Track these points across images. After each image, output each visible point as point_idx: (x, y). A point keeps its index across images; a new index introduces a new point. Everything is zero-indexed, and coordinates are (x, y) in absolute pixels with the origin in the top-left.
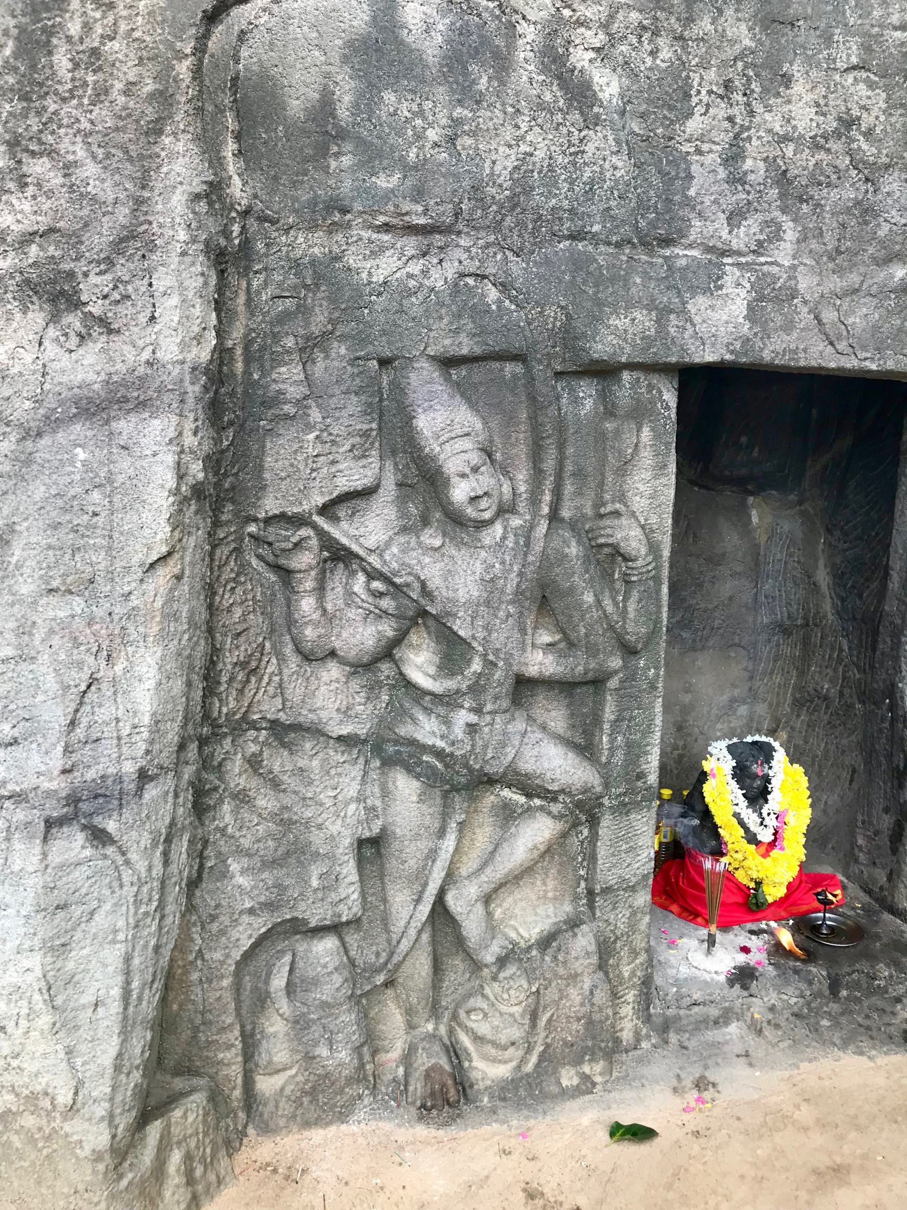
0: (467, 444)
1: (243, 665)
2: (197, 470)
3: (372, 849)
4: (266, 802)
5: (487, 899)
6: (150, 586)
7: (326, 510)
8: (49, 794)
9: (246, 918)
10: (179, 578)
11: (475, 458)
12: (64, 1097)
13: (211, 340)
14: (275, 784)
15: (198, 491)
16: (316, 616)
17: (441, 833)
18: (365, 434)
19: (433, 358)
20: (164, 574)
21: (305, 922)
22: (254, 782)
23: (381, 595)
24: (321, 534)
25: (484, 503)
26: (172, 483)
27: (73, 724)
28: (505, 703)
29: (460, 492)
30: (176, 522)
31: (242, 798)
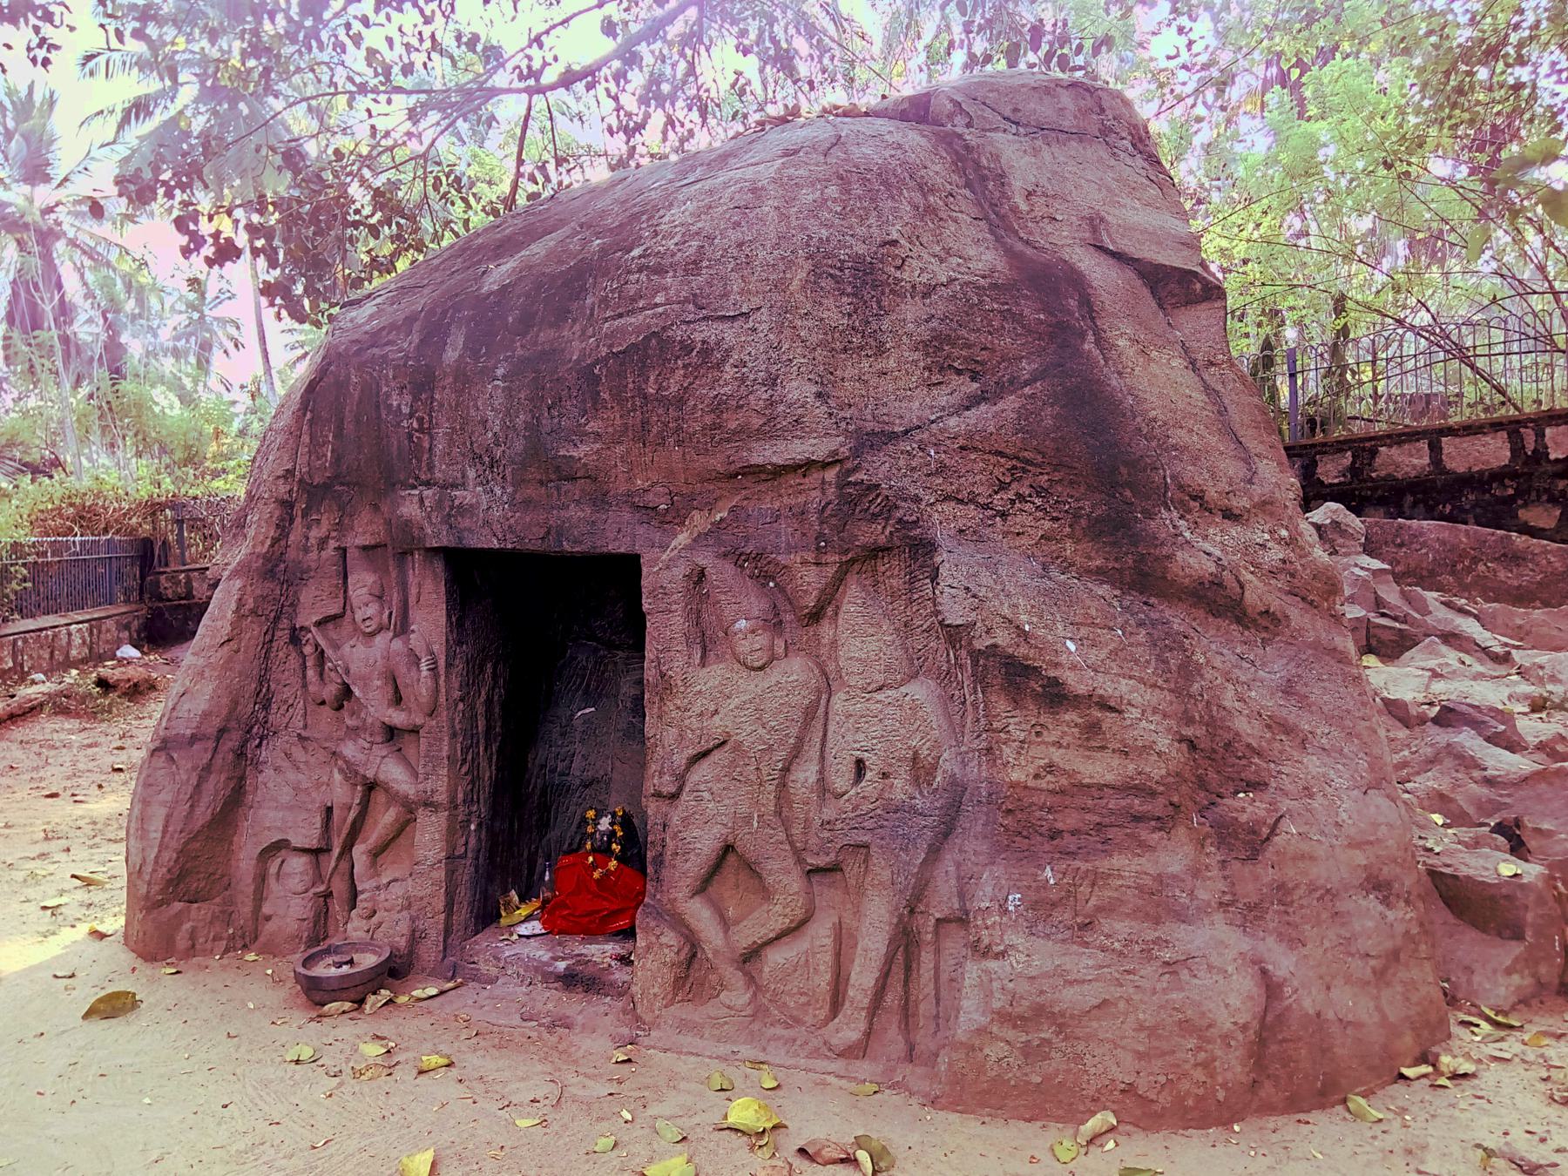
6: (219, 655)
7: (318, 624)
10: (237, 651)
11: (367, 598)
15: (253, 612)
20: (226, 648)
26: (233, 606)
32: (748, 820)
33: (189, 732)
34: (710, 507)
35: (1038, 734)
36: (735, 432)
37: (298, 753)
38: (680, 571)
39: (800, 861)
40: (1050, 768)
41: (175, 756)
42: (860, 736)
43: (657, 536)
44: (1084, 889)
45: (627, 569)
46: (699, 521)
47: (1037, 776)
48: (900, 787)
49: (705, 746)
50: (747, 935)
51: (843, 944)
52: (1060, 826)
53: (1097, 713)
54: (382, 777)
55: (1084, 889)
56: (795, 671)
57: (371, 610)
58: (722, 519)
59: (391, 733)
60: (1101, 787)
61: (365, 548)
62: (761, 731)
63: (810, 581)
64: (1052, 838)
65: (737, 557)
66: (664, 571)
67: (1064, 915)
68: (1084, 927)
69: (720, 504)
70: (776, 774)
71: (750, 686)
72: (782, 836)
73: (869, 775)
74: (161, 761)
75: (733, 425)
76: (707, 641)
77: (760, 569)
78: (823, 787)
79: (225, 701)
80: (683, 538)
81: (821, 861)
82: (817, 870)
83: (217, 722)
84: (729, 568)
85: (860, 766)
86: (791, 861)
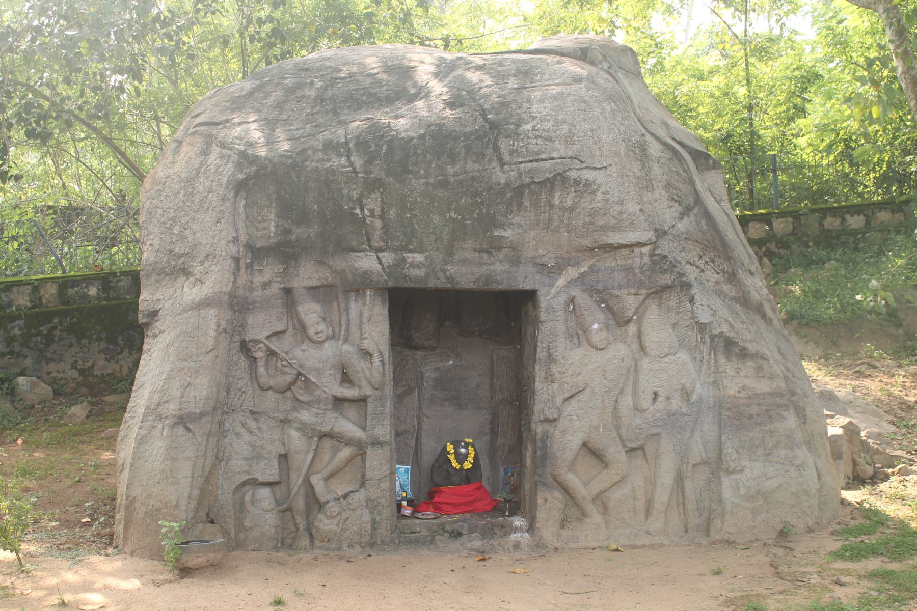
0: (315, 315)
1: (240, 389)
2: (223, 324)
3: (284, 458)
4: (247, 437)
5: (327, 479)
7: (268, 337)
8: (174, 416)
9: (237, 475)
12: (174, 503)
13: (231, 284)
14: (251, 432)
15: (225, 330)
16: (265, 374)
17: (307, 453)
18: (282, 313)
19: (304, 288)
20: (211, 354)
21: (257, 479)
22: (243, 430)
23: (285, 366)
24: (266, 346)
25: (320, 335)
27: (182, 396)
28: (330, 407)
29: (311, 331)
30: (216, 339)
31: (237, 434)
32: (597, 428)
33: (197, 411)
34: (577, 264)
35: (738, 373)
36: (602, 227)
37: (252, 424)
38: (562, 299)
39: (624, 446)
40: (744, 388)
41: (191, 427)
42: (656, 380)
43: (546, 280)
44: (767, 438)
45: (530, 296)
46: (572, 272)
47: (739, 392)
48: (676, 403)
49: (574, 391)
50: (596, 487)
51: (652, 483)
52: (752, 412)
53: (760, 361)
54: (336, 430)
55: (767, 438)
56: (621, 351)
57: (322, 327)
58: (585, 272)
59: (339, 402)
60: (764, 394)
61: (310, 288)
62: (605, 382)
63: (631, 302)
64: (750, 418)
65: (591, 291)
66: (552, 298)
67: (760, 451)
68: (768, 455)
69: (583, 263)
70: (612, 403)
71: (597, 359)
72: (615, 435)
73: (660, 399)
74: (181, 430)
75: (601, 223)
76: (579, 334)
77: (604, 298)
78: (638, 409)
79: (215, 389)
80: (561, 282)
81: (634, 445)
82: (633, 449)
83: (212, 404)
84: (586, 296)
85: (655, 395)
86: (621, 446)
